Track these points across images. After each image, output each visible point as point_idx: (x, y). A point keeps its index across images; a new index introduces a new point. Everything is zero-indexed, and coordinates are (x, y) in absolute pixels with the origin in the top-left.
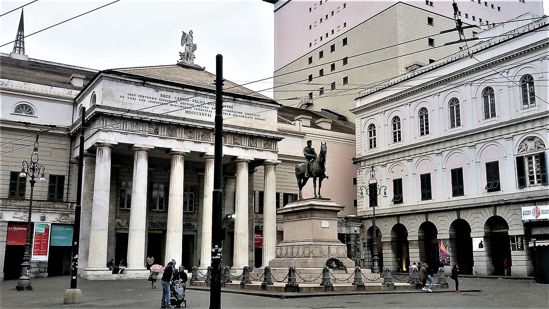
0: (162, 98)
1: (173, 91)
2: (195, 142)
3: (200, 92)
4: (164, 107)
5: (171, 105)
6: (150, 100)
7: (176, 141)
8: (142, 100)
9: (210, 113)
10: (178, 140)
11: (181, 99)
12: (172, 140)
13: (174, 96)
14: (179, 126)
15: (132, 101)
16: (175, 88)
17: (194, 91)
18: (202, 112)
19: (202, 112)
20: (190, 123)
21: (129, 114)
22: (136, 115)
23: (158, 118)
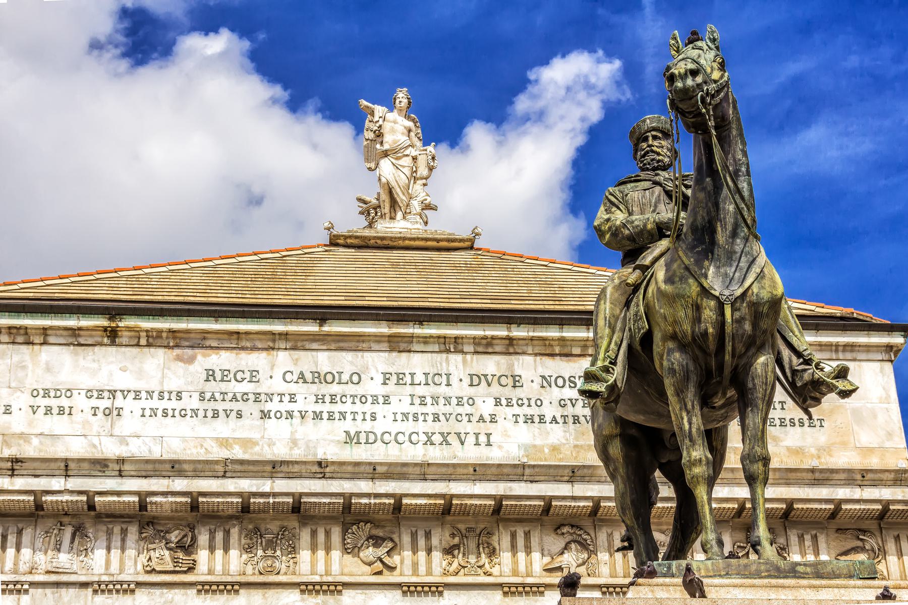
0: (213, 387)
1: (272, 342)
2: (408, 589)
3: (417, 330)
4: (224, 428)
5: (265, 415)
6: (149, 404)
7: (293, 596)
8: (108, 413)
9: (483, 428)
10: (307, 588)
11: (319, 378)
12: (271, 593)
13: (274, 369)
14: (298, 509)
15: (57, 424)
16: (278, 327)
17: (383, 329)
18: (442, 426)
19: (442, 426)
20: (364, 486)
21: (20, 483)
22: (57, 483)
23: (180, 484)
